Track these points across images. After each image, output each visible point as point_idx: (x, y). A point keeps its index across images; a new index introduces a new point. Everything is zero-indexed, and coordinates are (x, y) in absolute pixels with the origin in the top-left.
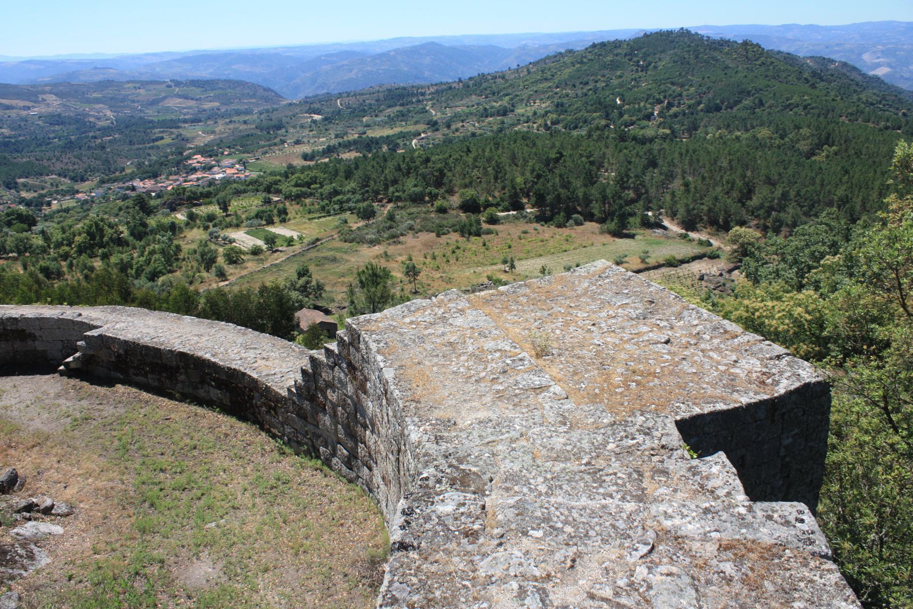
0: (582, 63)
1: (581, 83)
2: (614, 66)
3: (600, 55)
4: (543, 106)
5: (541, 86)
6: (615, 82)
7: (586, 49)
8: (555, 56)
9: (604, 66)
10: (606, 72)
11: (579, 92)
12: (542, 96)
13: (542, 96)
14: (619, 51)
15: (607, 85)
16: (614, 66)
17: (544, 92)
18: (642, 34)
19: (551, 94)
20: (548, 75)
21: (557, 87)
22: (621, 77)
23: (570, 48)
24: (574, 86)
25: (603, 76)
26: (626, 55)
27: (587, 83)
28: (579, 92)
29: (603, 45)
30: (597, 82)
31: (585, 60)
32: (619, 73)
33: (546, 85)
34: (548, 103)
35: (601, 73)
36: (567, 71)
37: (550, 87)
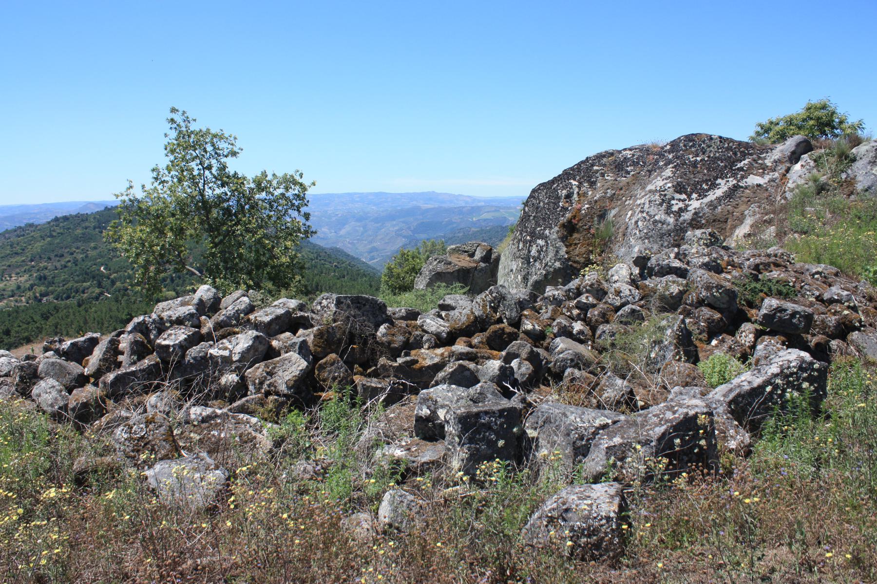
0: (51, 236)
1: (56, 256)
2: (86, 238)
3: (69, 228)
4: (22, 279)
5: (13, 260)
6: (92, 253)
7: (49, 223)
8: (15, 231)
9: (77, 239)
10: (79, 244)
11: (58, 265)
12: (18, 270)
13: (18, 270)
14: (87, 224)
15: (87, 257)
16: (86, 238)
17: (18, 267)
18: (103, 209)
19: (27, 267)
20: (18, 249)
21: (32, 261)
22: (95, 248)
23: (31, 222)
24: (50, 259)
25: (78, 248)
26: (95, 228)
27: (62, 256)
28: (58, 265)
29: (66, 218)
30: (72, 254)
31: (54, 234)
32: (92, 245)
33: (19, 259)
34: (26, 277)
35: (75, 245)
36: (38, 246)
37: (23, 261)
